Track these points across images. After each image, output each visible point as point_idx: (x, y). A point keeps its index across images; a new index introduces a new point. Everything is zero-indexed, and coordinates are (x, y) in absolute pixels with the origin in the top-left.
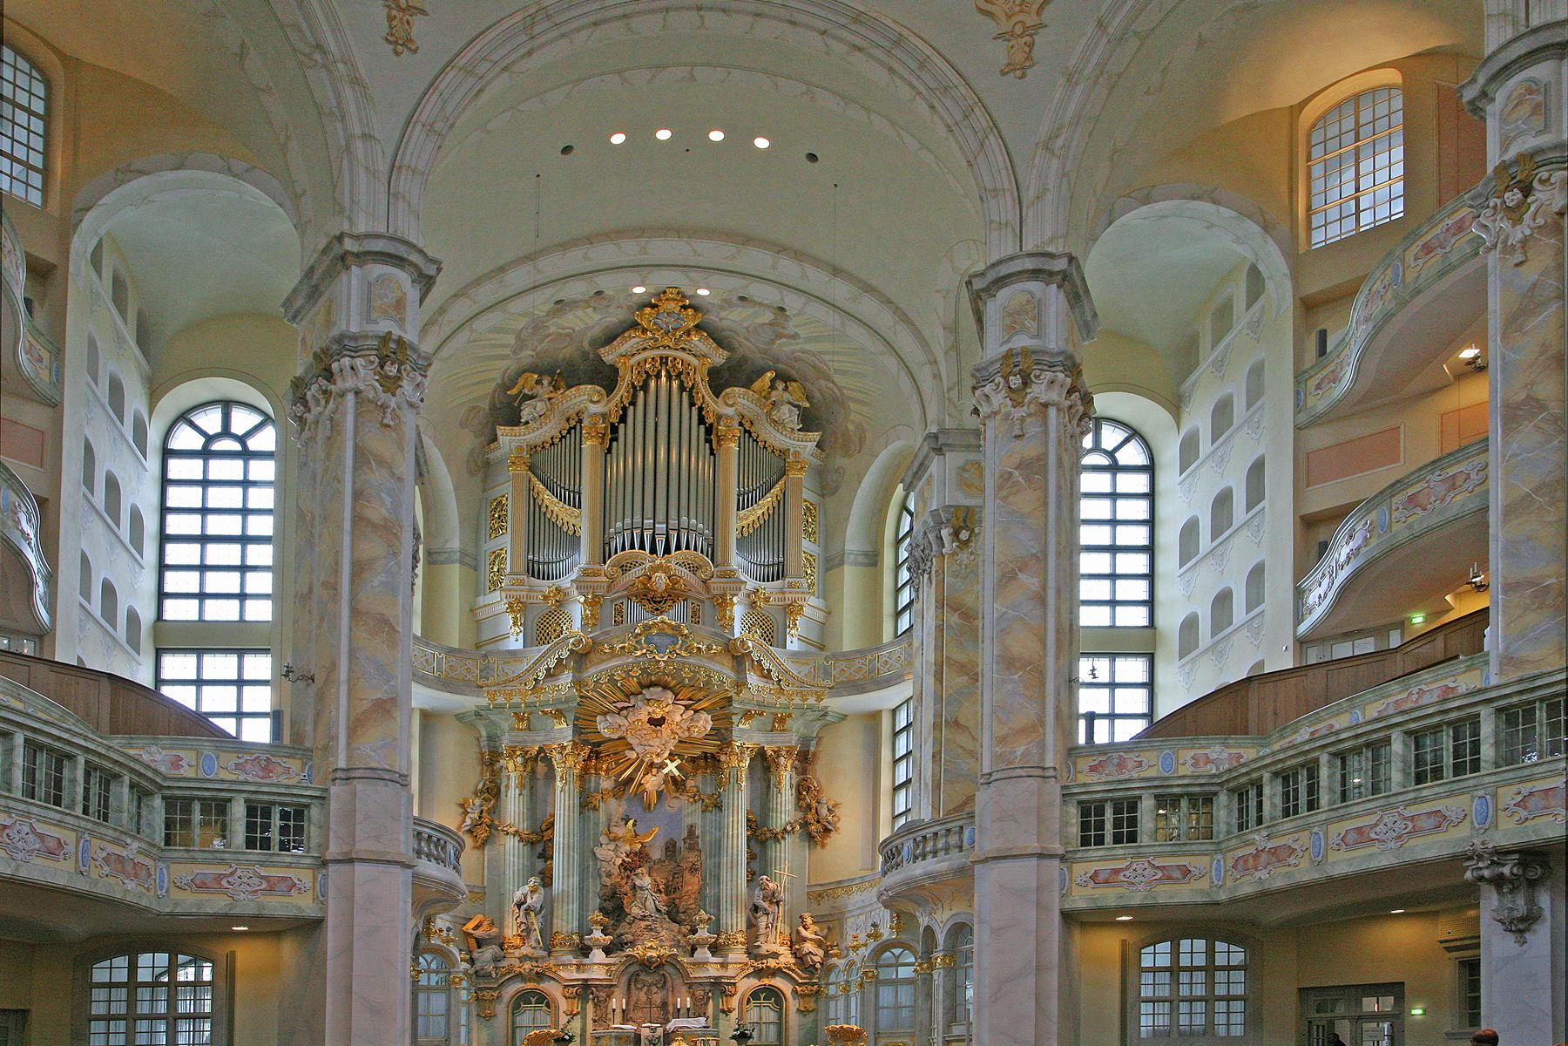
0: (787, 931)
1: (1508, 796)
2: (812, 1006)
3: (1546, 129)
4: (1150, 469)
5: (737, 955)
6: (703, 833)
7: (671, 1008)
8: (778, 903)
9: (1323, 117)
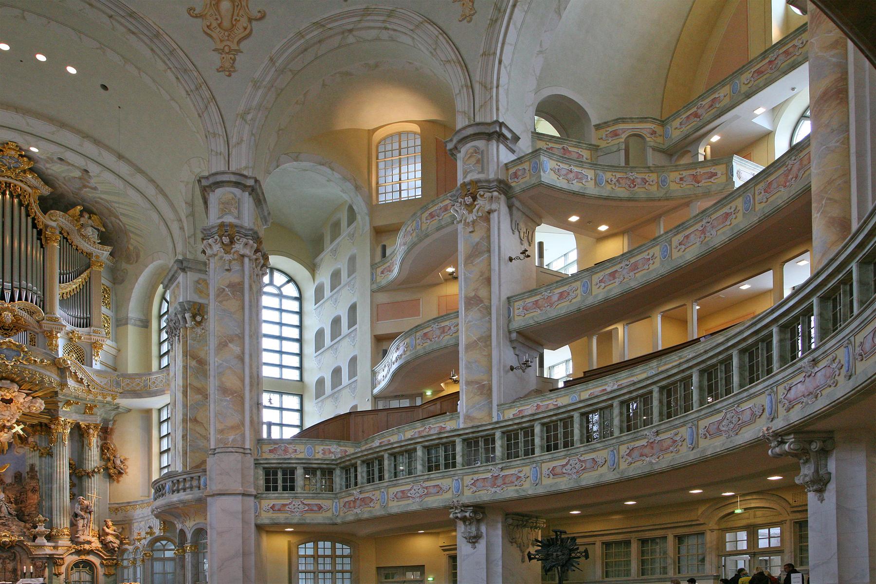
0: (97, 529)
1: (468, 480)
2: (113, 572)
3: (482, 172)
4: (300, 299)
5: (64, 542)
6: (41, 469)
7: (19, 573)
8: (90, 513)
9: (384, 139)
